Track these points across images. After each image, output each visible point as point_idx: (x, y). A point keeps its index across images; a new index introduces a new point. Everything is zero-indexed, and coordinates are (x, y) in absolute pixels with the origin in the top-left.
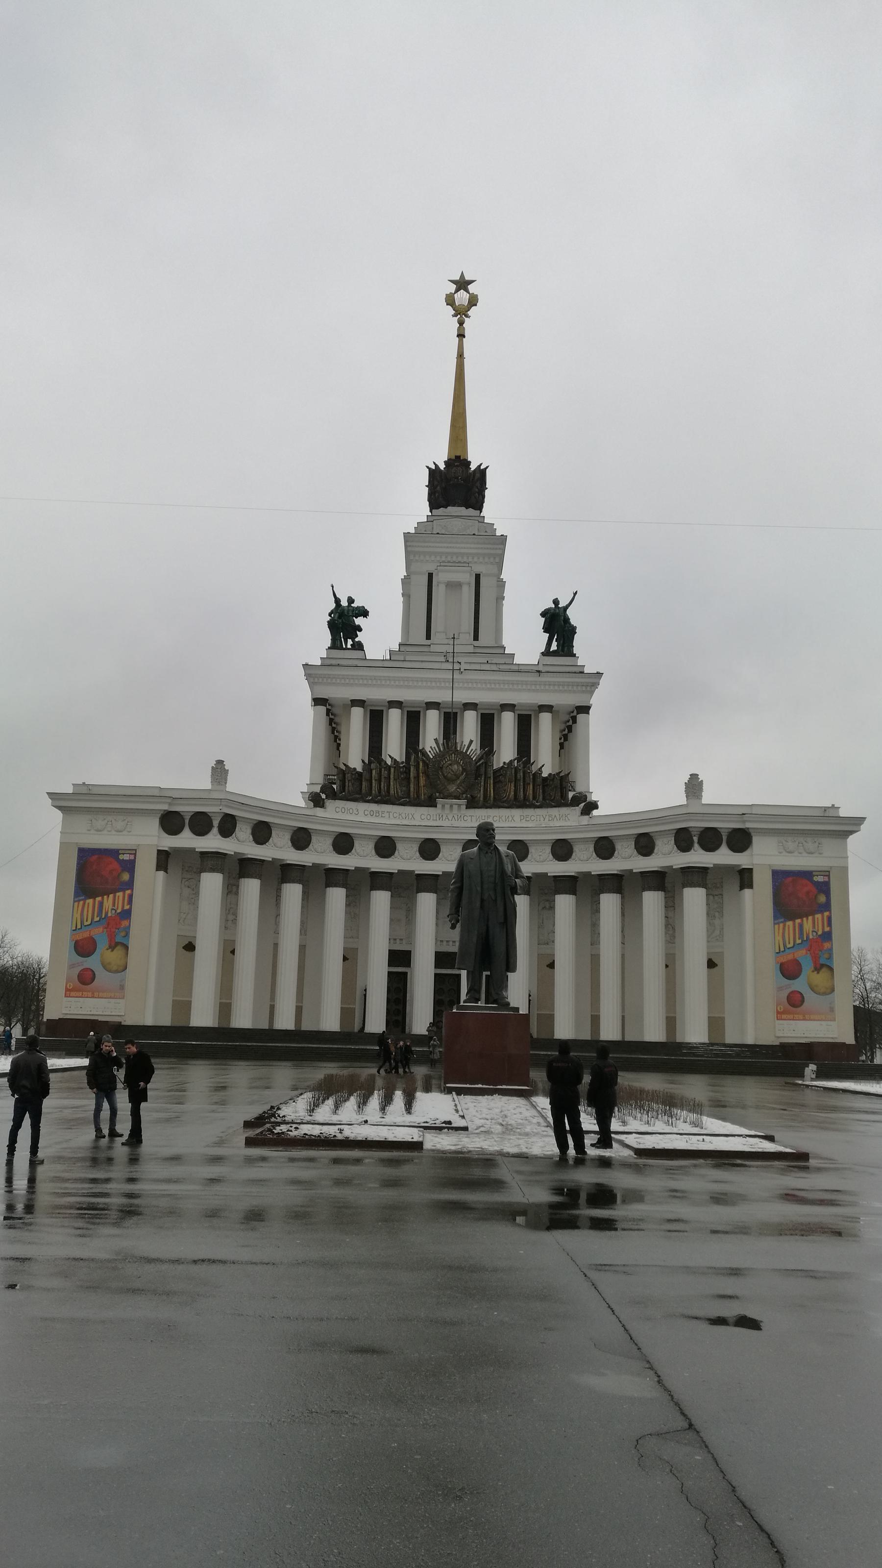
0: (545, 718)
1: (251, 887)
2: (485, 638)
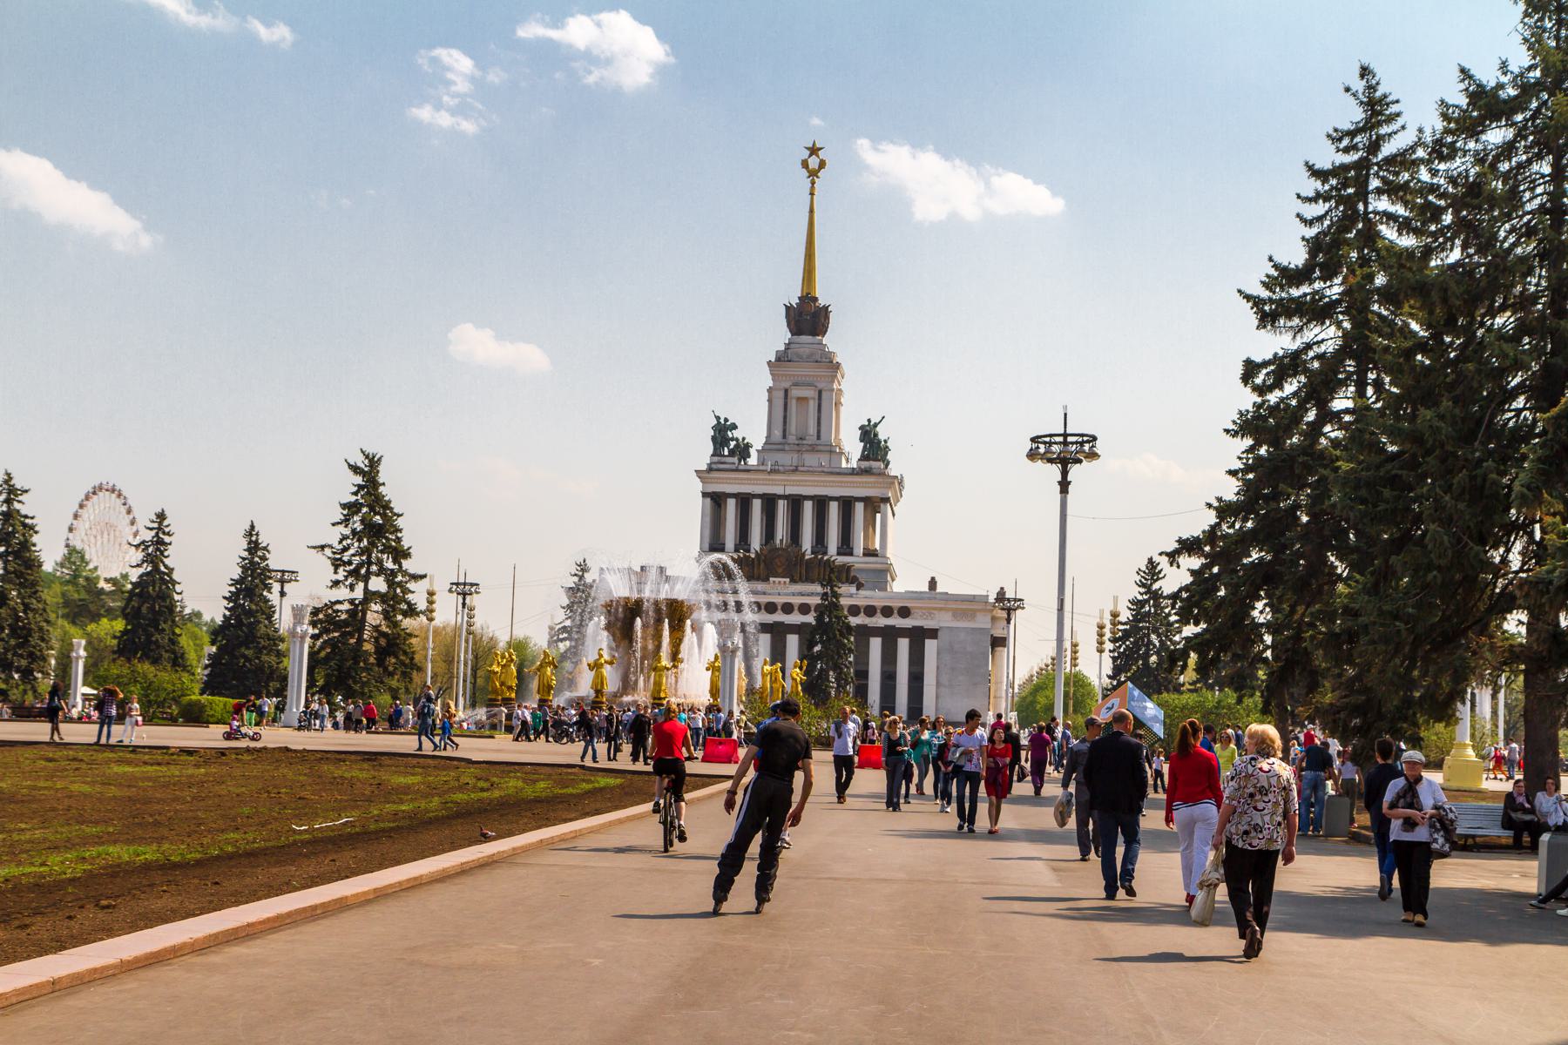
0: (859, 508)
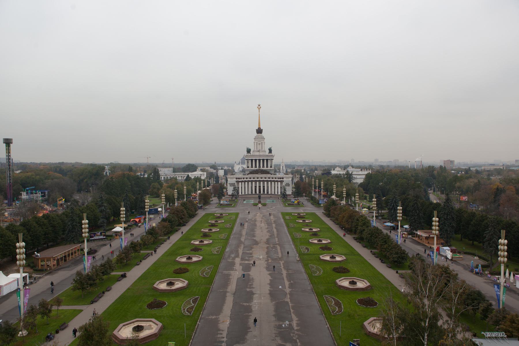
1: (243, 183)
2: (263, 149)
